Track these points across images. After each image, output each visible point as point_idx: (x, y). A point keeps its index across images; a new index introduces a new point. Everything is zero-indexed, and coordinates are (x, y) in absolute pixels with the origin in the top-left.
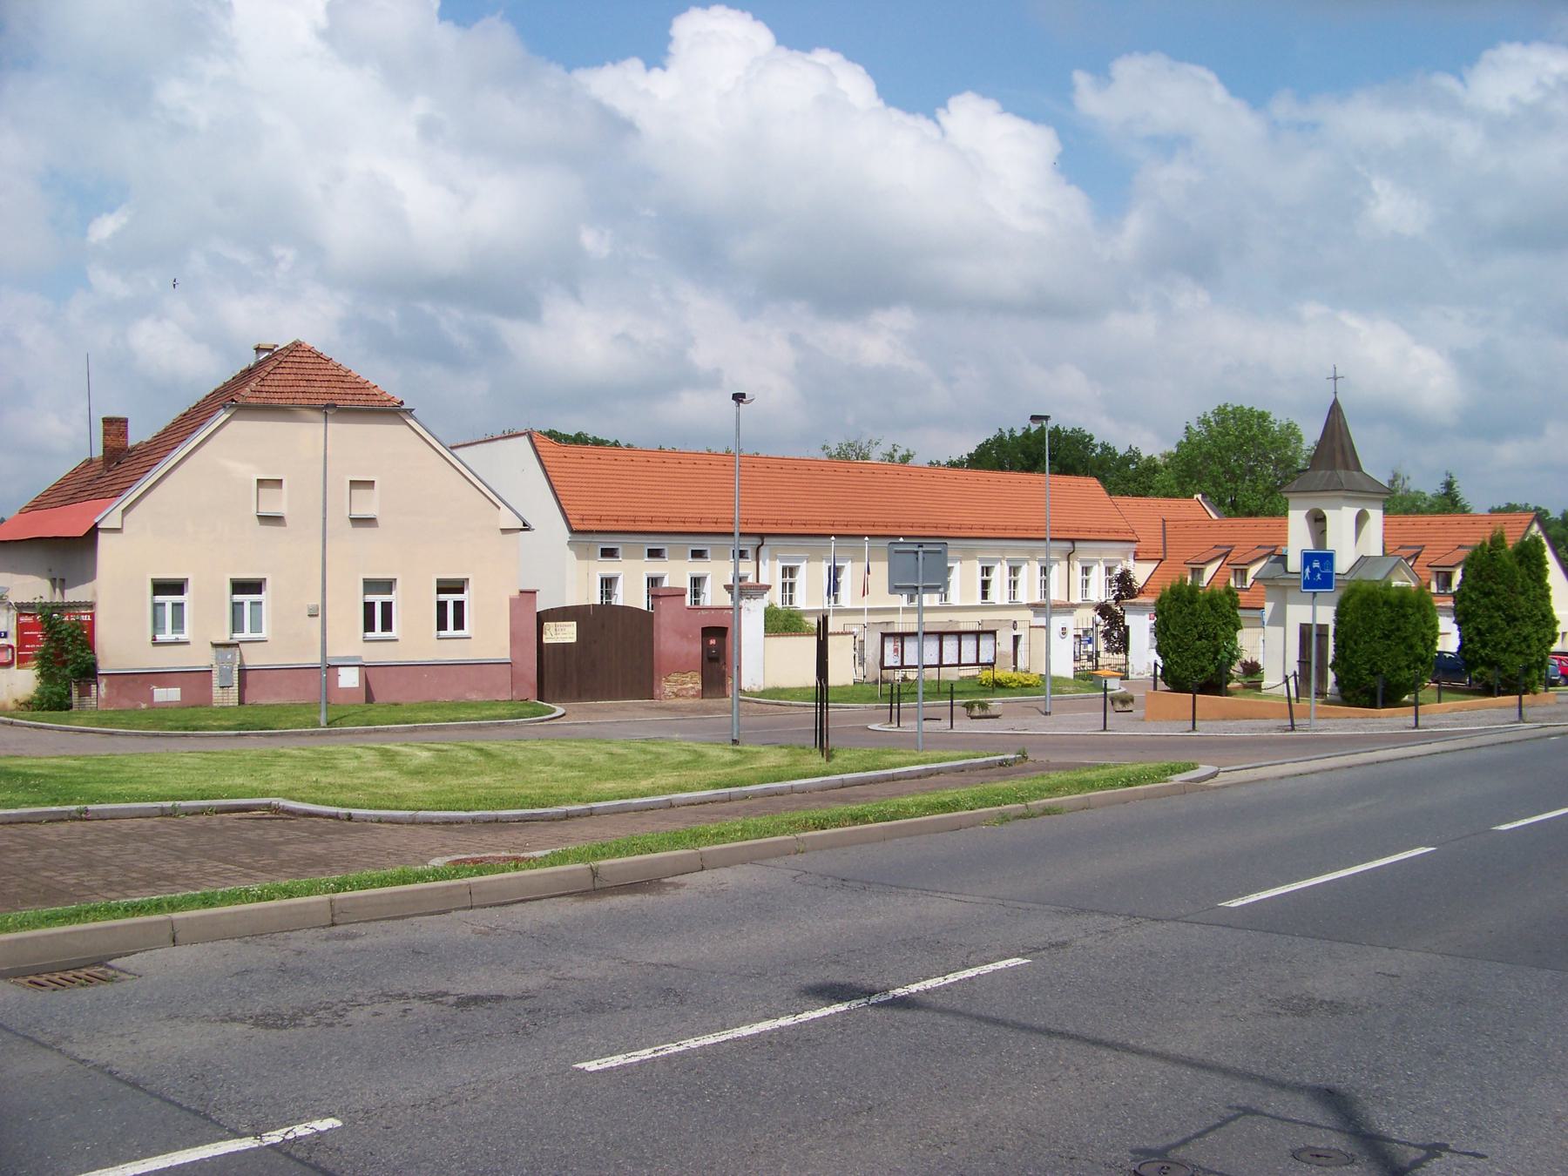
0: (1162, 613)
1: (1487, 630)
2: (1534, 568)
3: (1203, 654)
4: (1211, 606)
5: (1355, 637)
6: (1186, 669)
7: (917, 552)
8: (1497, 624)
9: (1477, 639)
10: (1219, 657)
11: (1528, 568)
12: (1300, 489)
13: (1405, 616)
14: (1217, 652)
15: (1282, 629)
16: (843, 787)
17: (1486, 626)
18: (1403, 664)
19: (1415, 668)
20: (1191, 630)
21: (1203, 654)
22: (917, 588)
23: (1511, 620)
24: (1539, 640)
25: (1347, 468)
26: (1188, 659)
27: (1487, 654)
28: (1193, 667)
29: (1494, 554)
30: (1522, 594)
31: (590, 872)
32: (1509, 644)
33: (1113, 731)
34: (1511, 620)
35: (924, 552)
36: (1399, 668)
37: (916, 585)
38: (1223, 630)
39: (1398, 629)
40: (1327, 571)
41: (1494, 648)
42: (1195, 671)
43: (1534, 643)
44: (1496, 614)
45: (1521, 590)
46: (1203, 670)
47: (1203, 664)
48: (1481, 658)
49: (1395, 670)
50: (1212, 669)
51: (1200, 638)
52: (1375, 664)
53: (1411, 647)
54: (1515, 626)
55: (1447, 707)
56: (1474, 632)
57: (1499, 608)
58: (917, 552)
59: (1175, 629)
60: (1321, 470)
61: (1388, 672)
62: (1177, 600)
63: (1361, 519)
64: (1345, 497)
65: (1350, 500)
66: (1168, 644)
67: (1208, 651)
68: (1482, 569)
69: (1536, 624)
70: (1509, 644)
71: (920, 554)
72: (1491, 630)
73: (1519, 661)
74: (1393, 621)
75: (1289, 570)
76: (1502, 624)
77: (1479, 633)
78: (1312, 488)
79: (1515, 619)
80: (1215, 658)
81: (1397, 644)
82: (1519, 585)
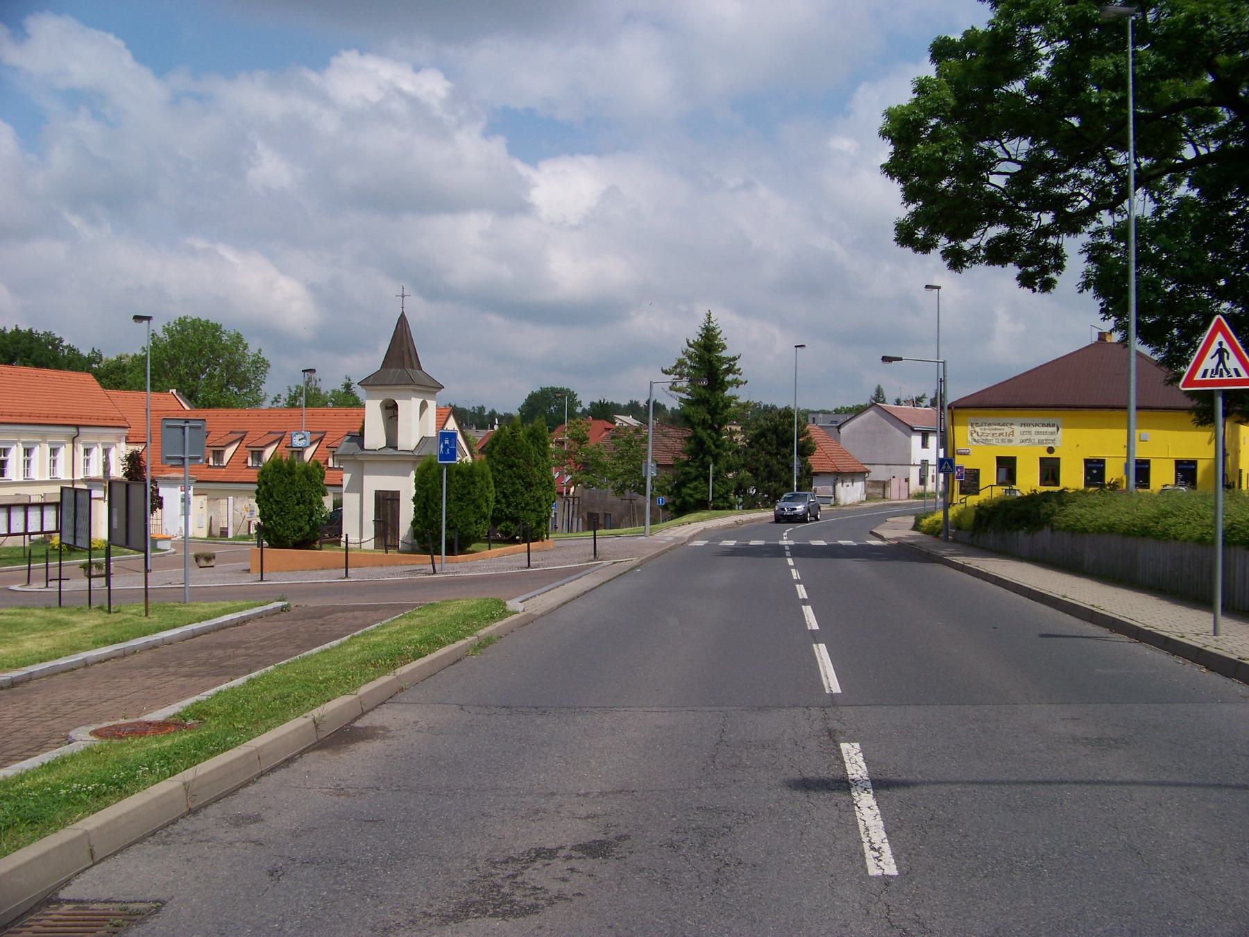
0: (266, 483)
1: (511, 493)
2: (541, 447)
3: (301, 516)
4: (307, 477)
5: (435, 500)
6: (288, 529)
7: (183, 428)
8: (518, 489)
9: (504, 501)
10: (314, 519)
11: (538, 447)
12: (376, 383)
13: (473, 483)
14: (311, 515)
15: (358, 495)
16: (194, 637)
17: (510, 490)
18: (473, 520)
19: (480, 523)
20: (291, 497)
21: (301, 516)
22: (183, 459)
23: (529, 486)
24: (546, 500)
25: (413, 368)
26: (289, 521)
27: (510, 512)
28: (293, 527)
29: (515, 436)
30: (535, 466)
31: (313, 724)
32: (527, 504)
33: (269, 581)
34: (529, 486)
35: (191, 427)
36: (471, 524)
37: (182, 456)
38: (315, 496)
39: (469, 493)
40: (453, 447)
41: (516, 507)
42: (294, 530)
43: (544, 503)
44: (517, 482)
45: (534, 463)
46: (301, 529)
47: (301, 525)
48: (506, 515)
49: (467, 526)
50: (307, 528)
51: (298, 504)
52: (452, 520)
53: (479, 507)
54: (531, 491)
55: (494, 553)
56: (501, 496)
57: (520, 477)
58: (183, 428)
59: (278, 496)
60: (392, 368)
61: (461, 527)
62: (279, 472)
63: (423, 406)
64: (415, 390)
65: (417, 392)
66: (272, 509)
67: (305, 514)
68: (506, 448)
69: (544, 488)
70: (527, 504)
71: (187, 429)
72: (514, 493)
73: (534, 516)
74: (464, 487)
75: (365, 447)
76: (522, 489)
77: (505, 496)
78: (387, 383)
79: (531, 485)
80: (310, 519)
81: (468, 505)
82: (533, 459)
